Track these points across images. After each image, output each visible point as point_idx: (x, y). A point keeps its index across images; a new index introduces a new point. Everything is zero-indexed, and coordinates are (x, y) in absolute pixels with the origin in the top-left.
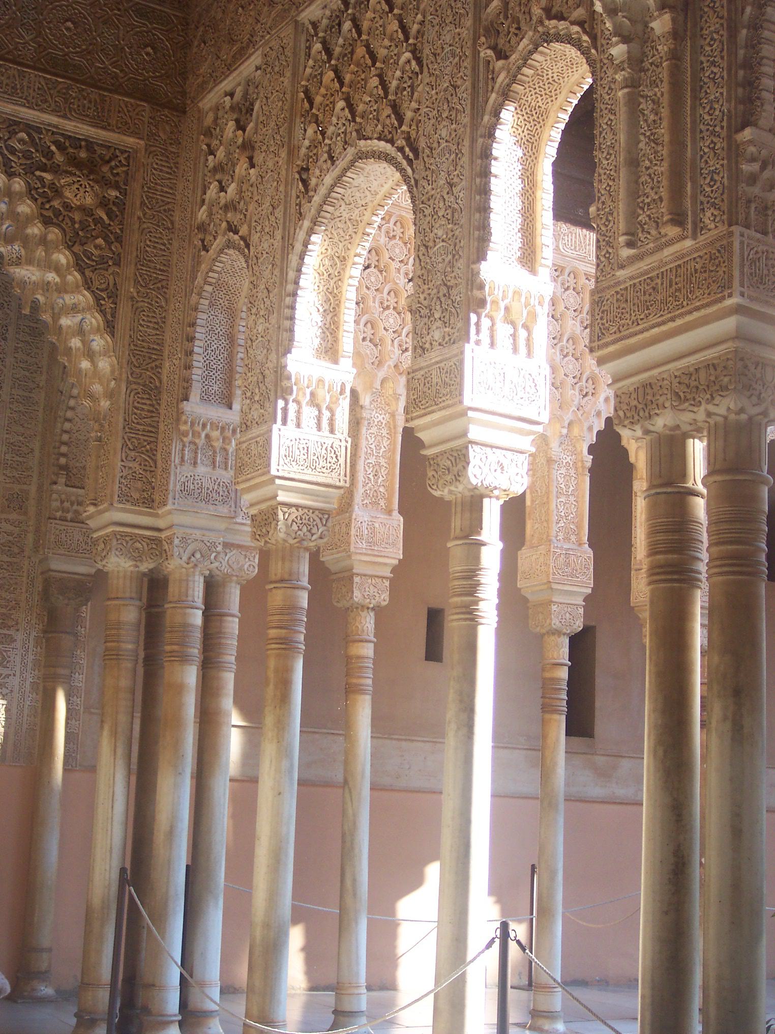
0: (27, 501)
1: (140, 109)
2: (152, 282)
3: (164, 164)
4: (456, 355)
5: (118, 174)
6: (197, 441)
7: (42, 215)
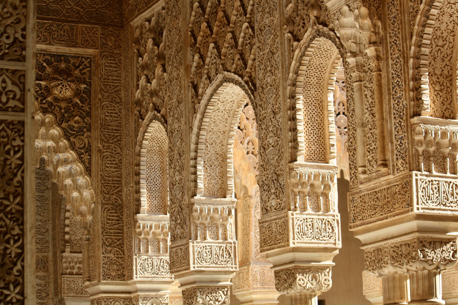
0: (47, 262)
1: (95, 29)
2: (111, 139)
3: (112, 62)
4: (284, 217)
5: (84, 73)
6: (147, 237)
7: (41, 107)
